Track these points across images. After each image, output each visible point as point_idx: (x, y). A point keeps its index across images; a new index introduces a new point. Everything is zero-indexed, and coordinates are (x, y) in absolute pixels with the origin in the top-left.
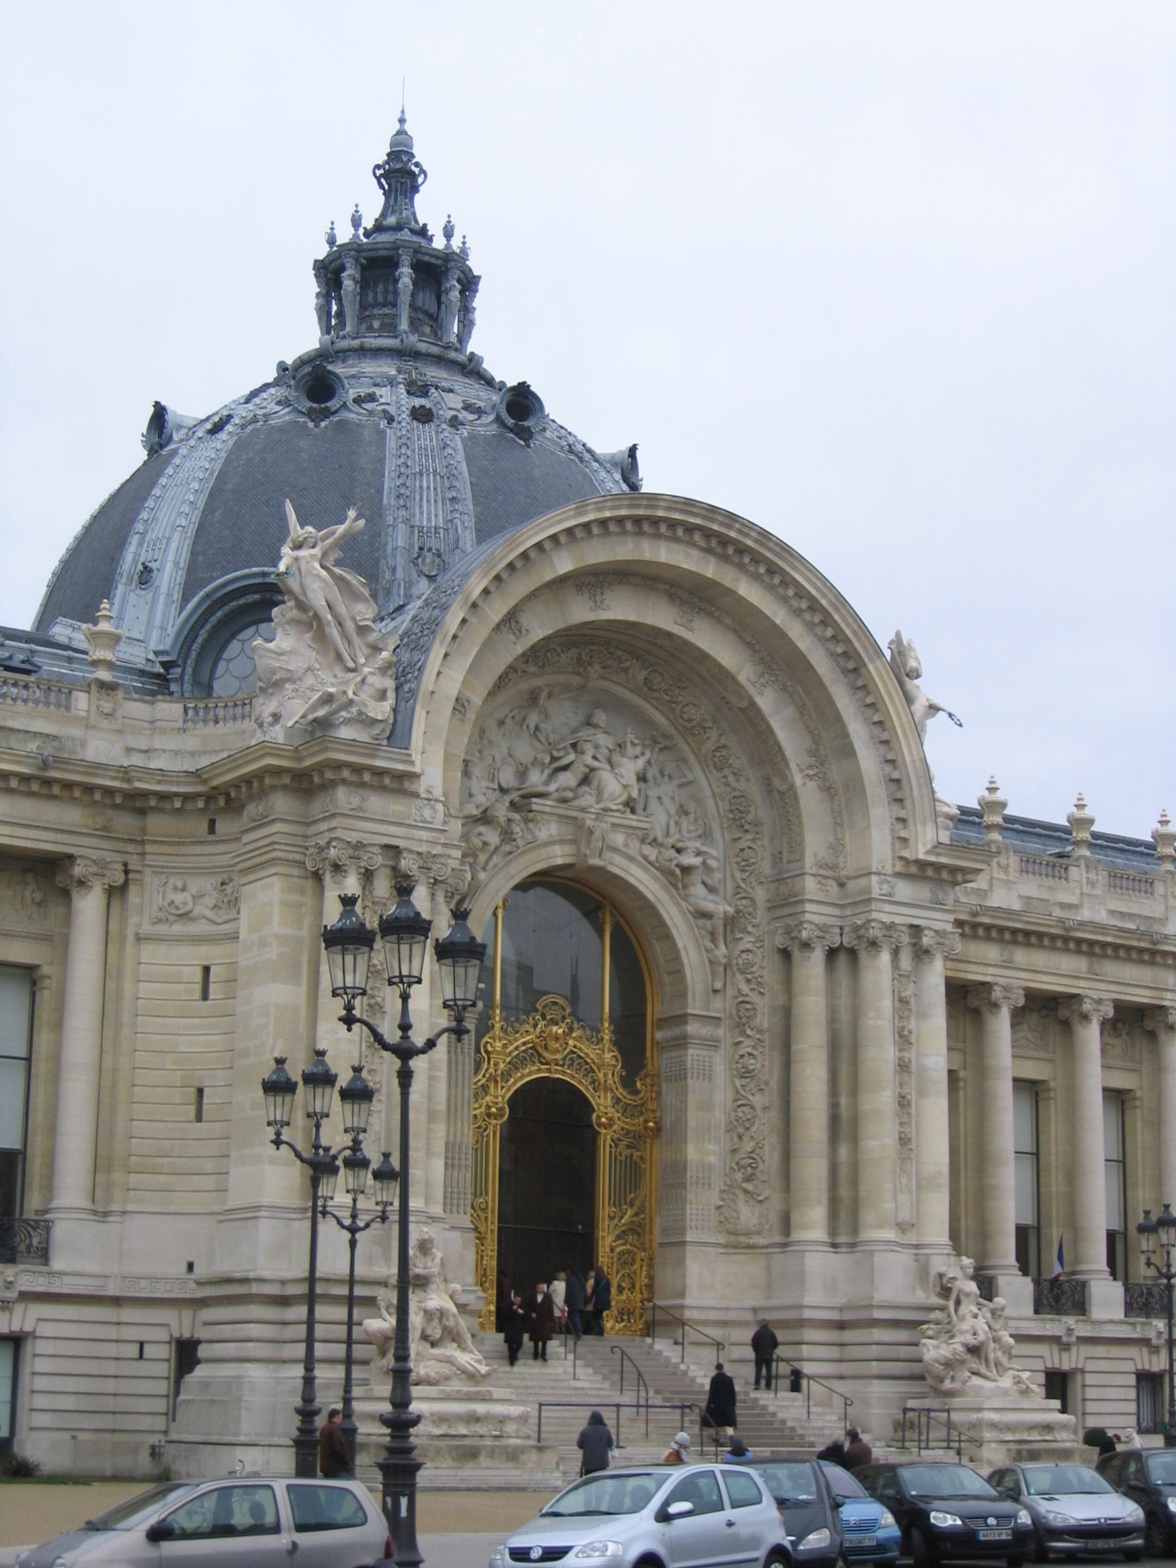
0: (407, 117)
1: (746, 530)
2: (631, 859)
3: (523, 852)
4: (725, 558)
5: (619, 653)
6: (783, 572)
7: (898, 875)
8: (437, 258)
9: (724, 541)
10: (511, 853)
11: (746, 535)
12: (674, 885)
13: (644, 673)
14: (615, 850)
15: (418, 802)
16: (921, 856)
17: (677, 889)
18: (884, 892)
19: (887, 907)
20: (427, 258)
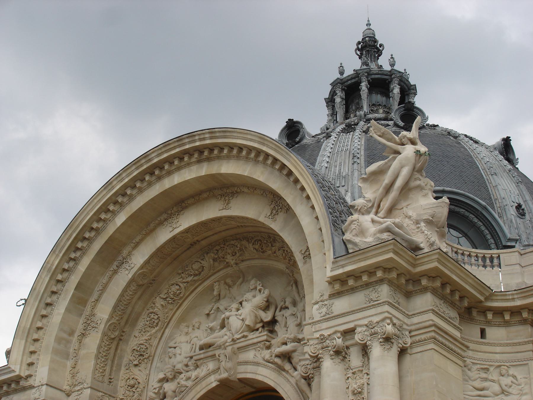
0: (370, 22)
1: (202, 137)
2: (257, 364)
3: (191, 388)
4: (209, 159)
5: (232, 242)
6: (235, 145)
7: (332, 296)
8: (354, 78)
9: (200, 150)
10: (183, 392)
11: (204, 139)
12: (284, 370)
13: (251, 245)
14: (246, 363)
15: (34, 390)
16: (329, 274)
17: (287, 372)
18: (322, 315)
19: (325, 325)
20: (349, 82)
